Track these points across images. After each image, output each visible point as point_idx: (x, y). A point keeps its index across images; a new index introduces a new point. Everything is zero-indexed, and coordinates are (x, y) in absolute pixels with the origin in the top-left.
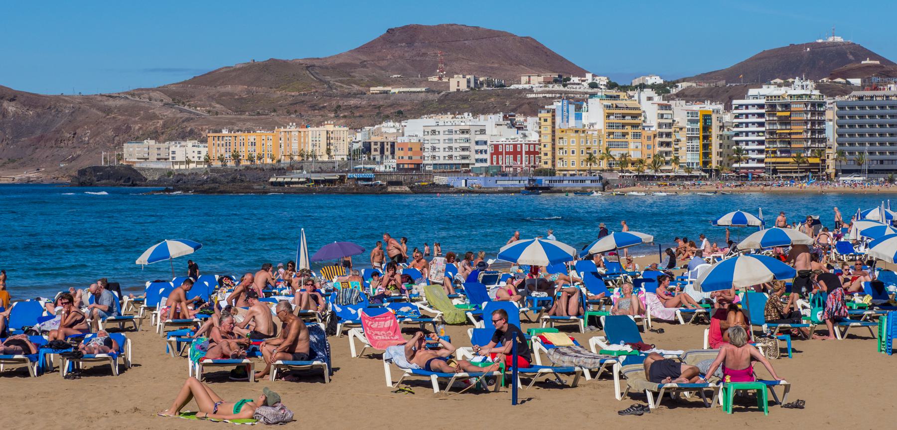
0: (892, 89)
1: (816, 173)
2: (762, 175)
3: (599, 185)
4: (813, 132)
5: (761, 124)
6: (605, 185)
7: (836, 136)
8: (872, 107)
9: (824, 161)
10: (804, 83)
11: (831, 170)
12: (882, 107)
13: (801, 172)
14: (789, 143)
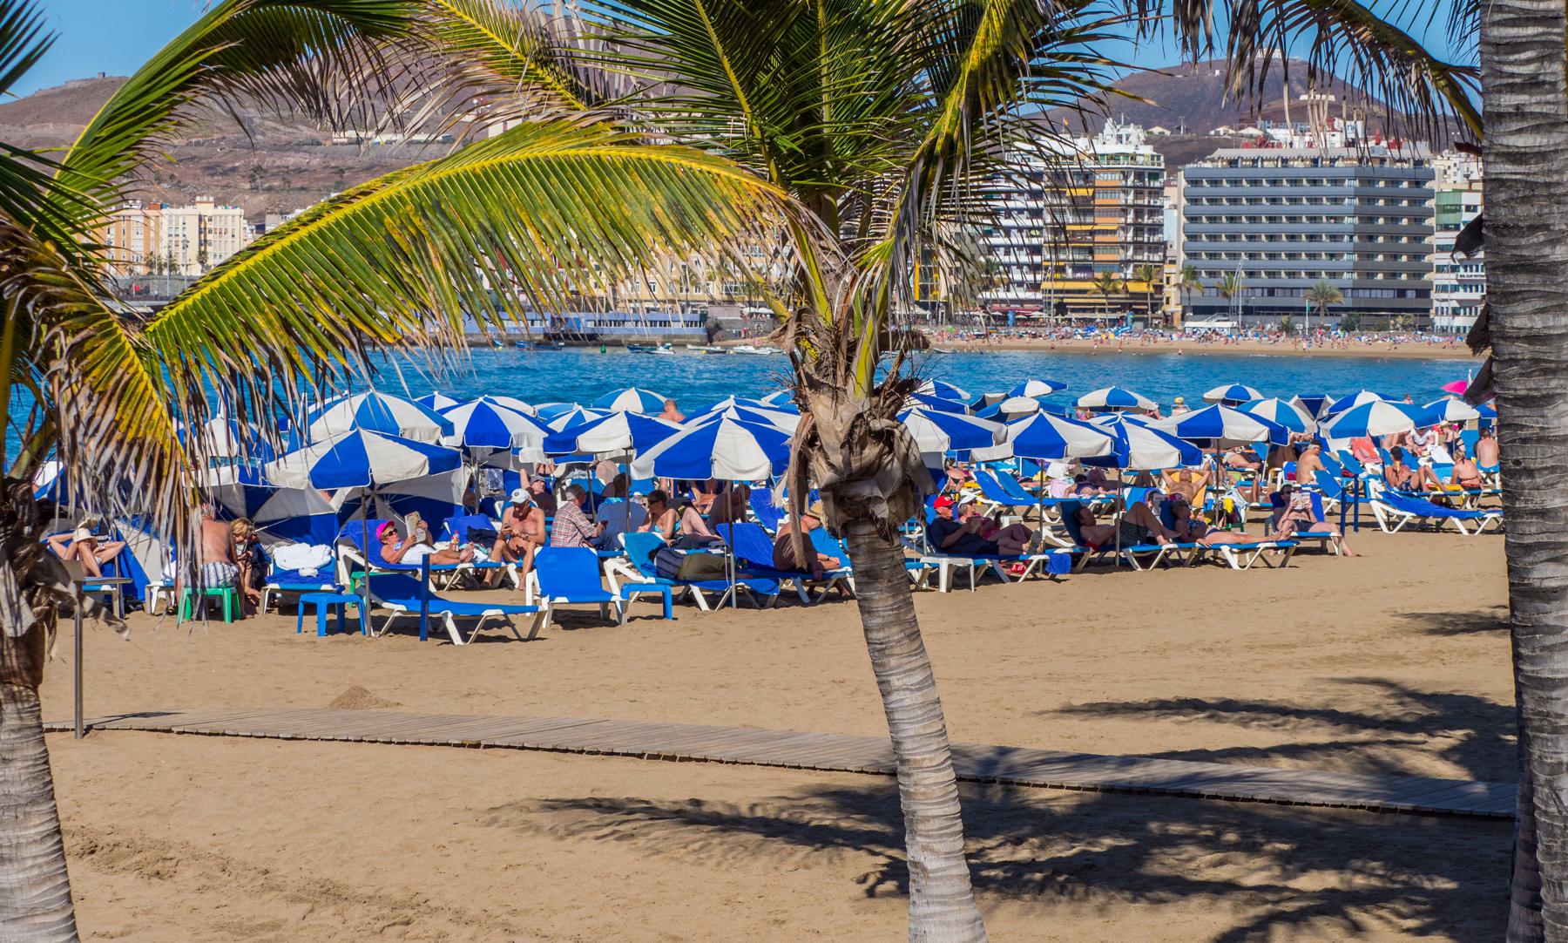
0: (1296, 145)
1: (1144, 311)
2: (1036, 314)
3: (700, 331)
4: (1139, 229)
5: (1036, 213)
6: (713, 333)
7: (1184, 238)
8: (1255, 182)
9: (1159, 288)
10: (1124, 132)
11: (1174, 307)
12: (1274, 182)
13: (1114, 311)
14: (1091, 251)
